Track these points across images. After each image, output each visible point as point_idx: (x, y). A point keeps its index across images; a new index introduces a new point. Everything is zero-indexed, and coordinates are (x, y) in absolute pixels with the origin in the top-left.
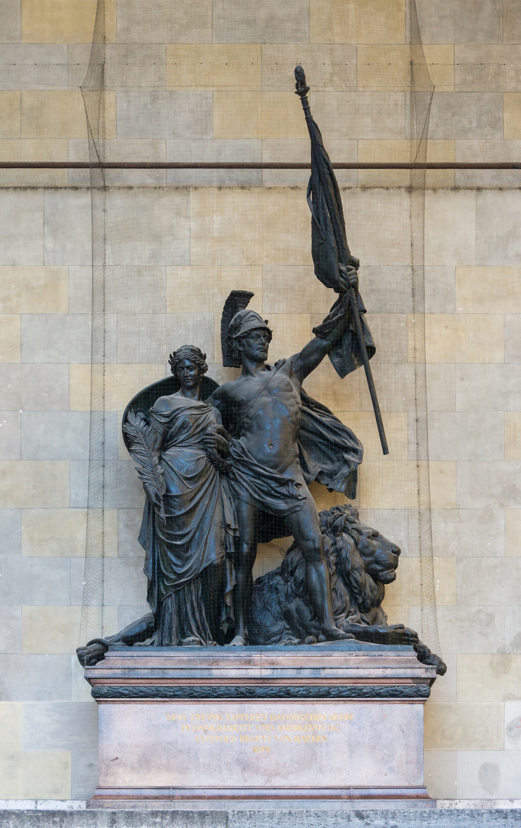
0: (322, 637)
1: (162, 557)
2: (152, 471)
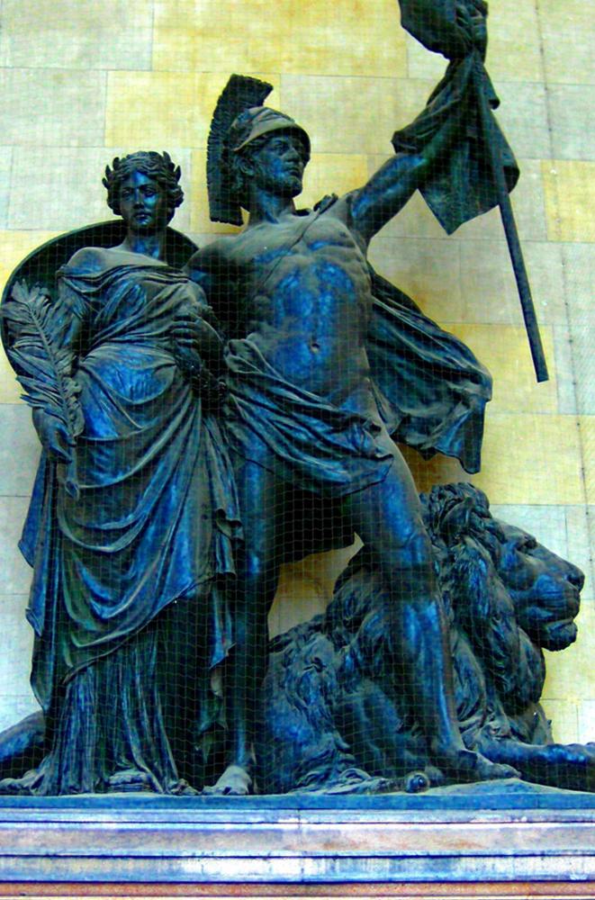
0: (435, 772)
1: (68, 584)
2: (55, 386)
